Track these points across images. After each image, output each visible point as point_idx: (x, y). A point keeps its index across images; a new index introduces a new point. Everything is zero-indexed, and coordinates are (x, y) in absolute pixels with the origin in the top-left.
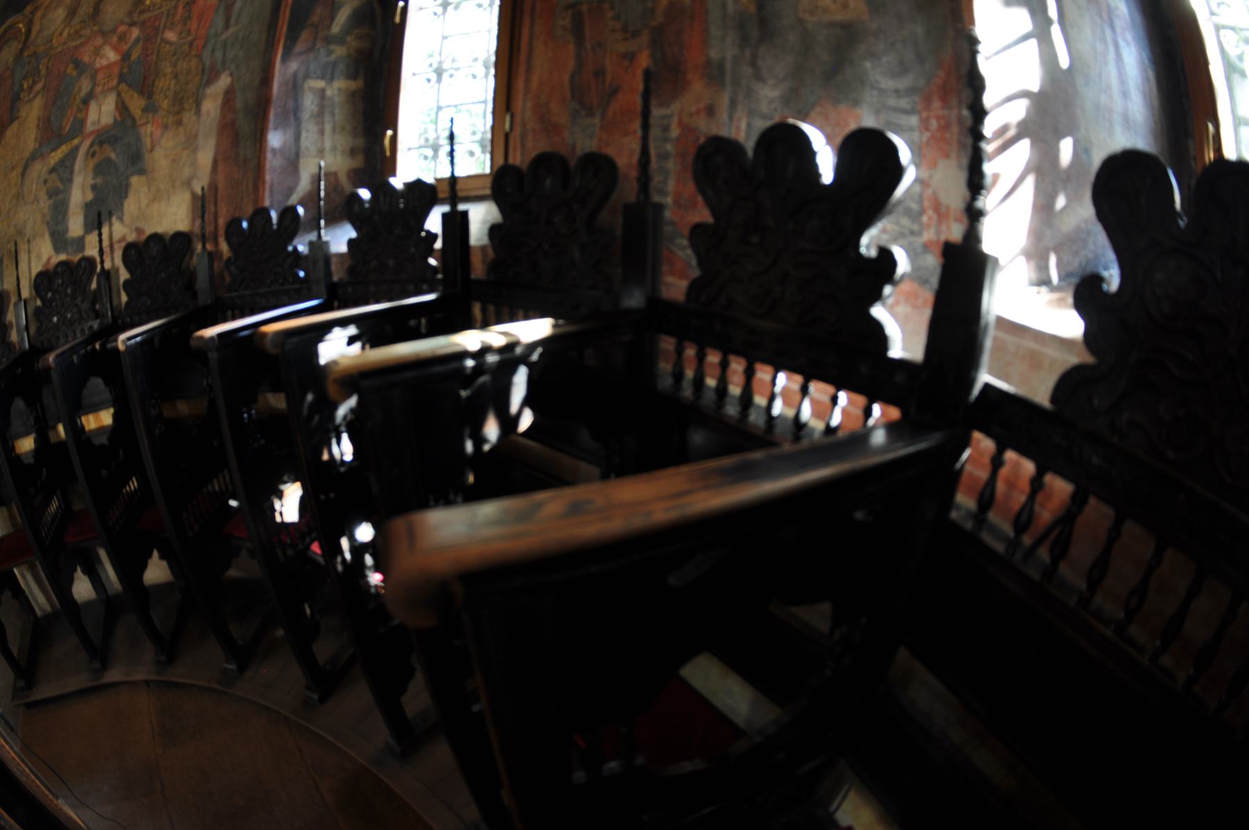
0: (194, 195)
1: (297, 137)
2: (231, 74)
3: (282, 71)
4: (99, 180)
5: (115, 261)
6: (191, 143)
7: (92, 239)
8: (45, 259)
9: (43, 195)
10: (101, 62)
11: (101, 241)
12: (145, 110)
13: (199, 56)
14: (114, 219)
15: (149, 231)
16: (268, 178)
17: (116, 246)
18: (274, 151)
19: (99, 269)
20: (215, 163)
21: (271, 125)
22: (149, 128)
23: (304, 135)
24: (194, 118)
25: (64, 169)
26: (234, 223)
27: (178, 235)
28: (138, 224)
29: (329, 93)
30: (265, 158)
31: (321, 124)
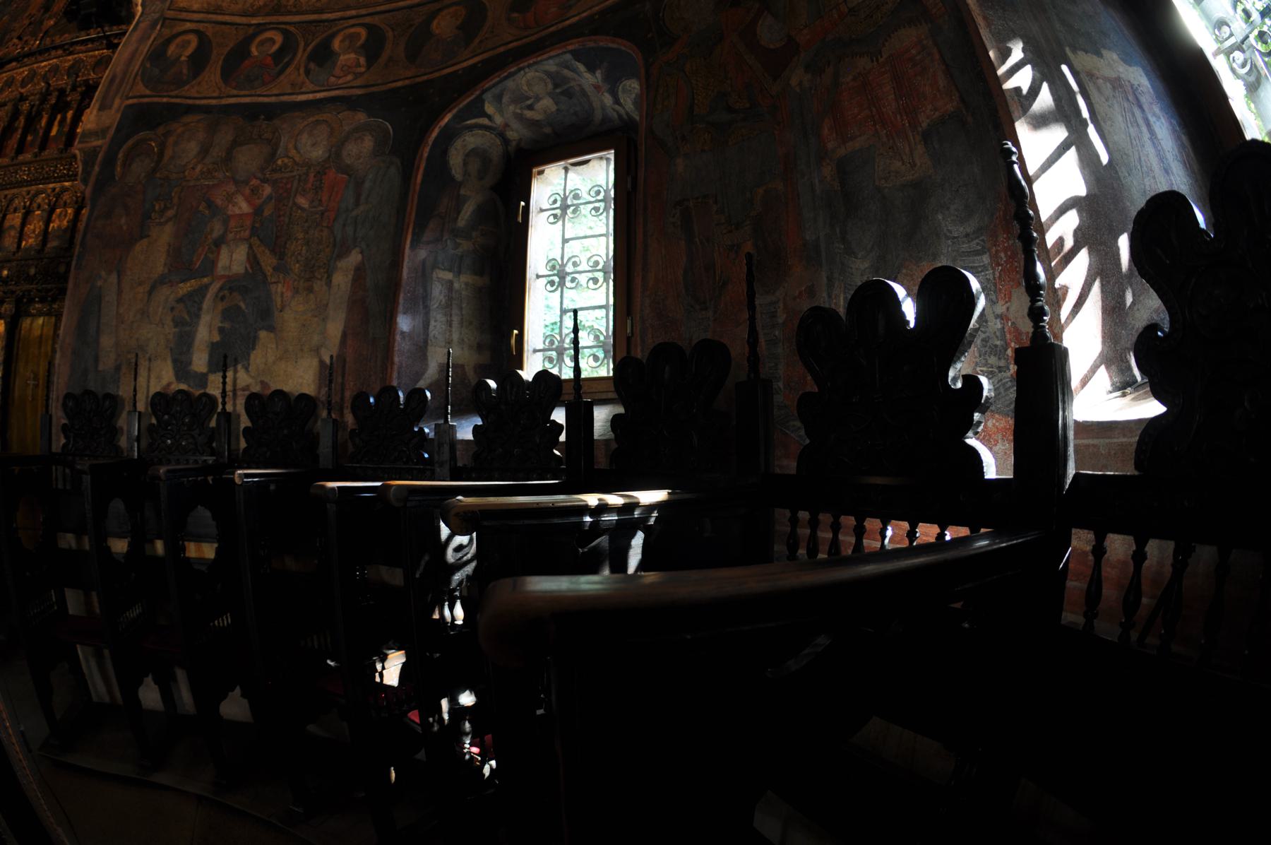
0: (322, 362)
1: (426, 325)
3: (414, 256)
4: (227, 325)
5: (238, 406)
6: (321, 311)
7: (215, 379)
11: (224, 383)
12: (275, 269)
14: (239, 367)
15: (275, 386)
17: (239, 393)
18: (403, 333)
20: (344, 335)
21: (401, 308)
22: (280, 288)
23: (432, 323)
26: (361, 397)
27: (303, 396)
29: (456, 285)
30: (394, 340)
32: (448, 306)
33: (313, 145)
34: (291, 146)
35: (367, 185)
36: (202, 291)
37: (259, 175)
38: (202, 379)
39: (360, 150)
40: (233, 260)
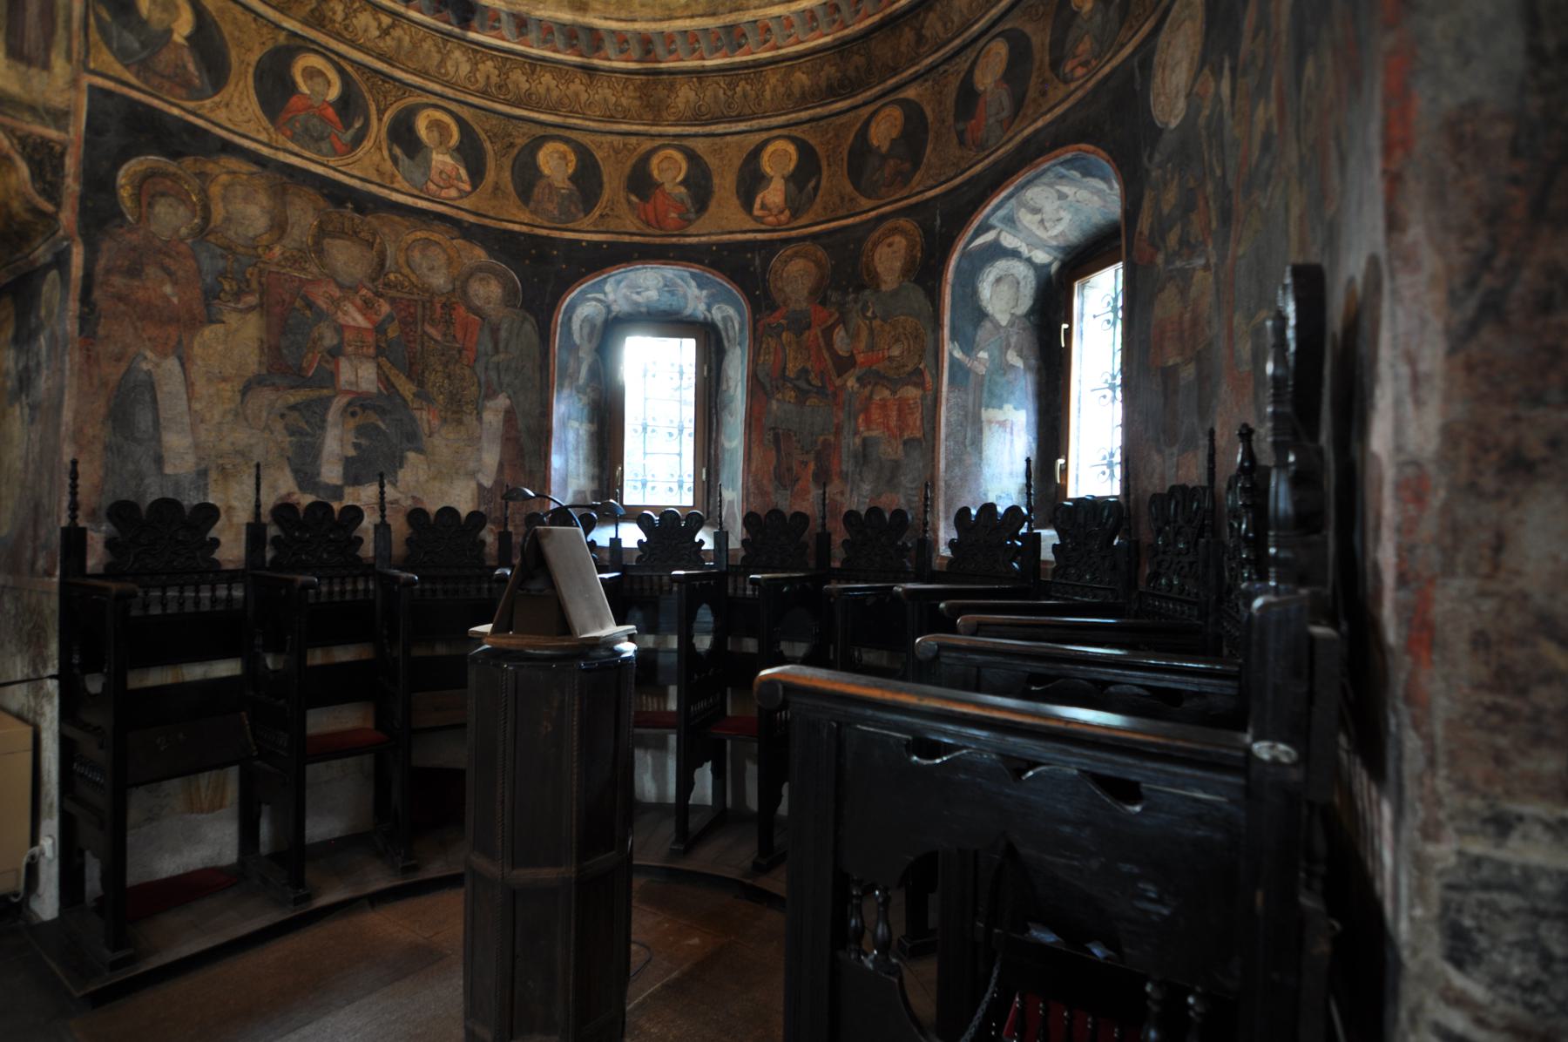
4: (363, 442)
9: (279, 426)
25: (314, 413)
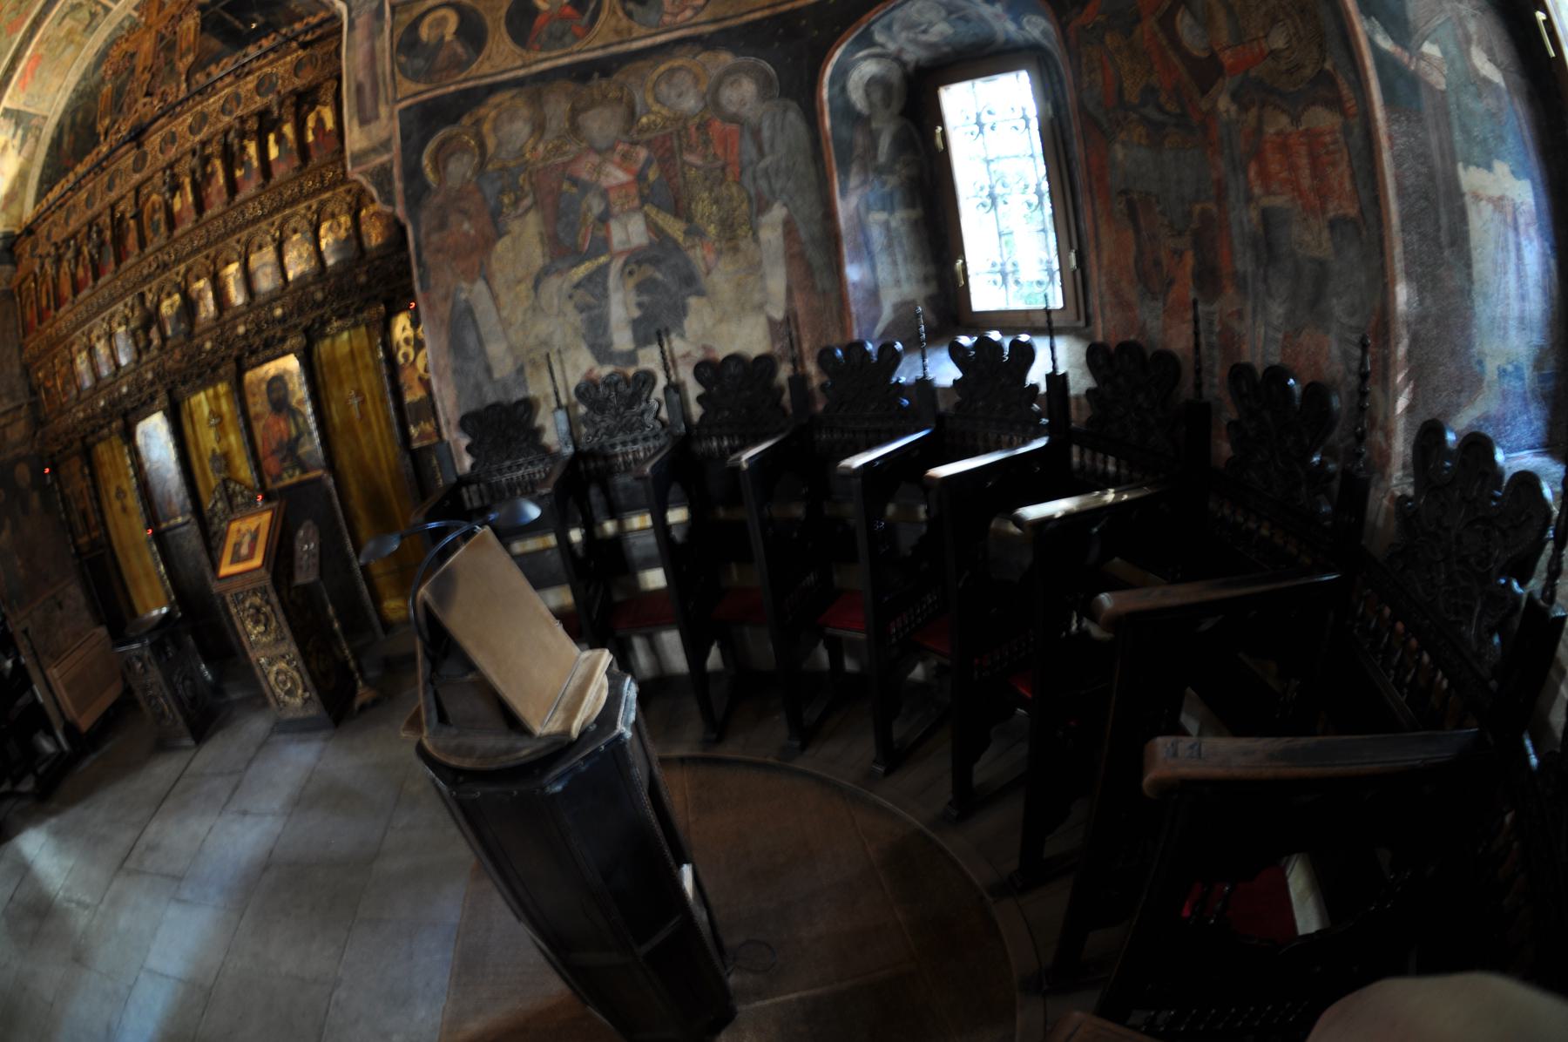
1: (873, 268)
2: (785, 205)
3: (845, 208)
4: (645, 299)
6: (755, 268)
8: (584, 368)
10: (612, 182)
12: (687, 233)
13: (739, 182)
14: (673, 336)
16: (853, 309)
19: (662, 381)
21: (846, 259)
24: (753, 246)
28: (709, 343)
29: (893, 224)
31: (892, 255)
32: (889, 246)
33: (680, 95)
34: (650, 101)
35: (766, 134)
36: (603, 271)
37: (625, 138)
38: (631, 358)
39: (742, 94)
40: (630, 232)
